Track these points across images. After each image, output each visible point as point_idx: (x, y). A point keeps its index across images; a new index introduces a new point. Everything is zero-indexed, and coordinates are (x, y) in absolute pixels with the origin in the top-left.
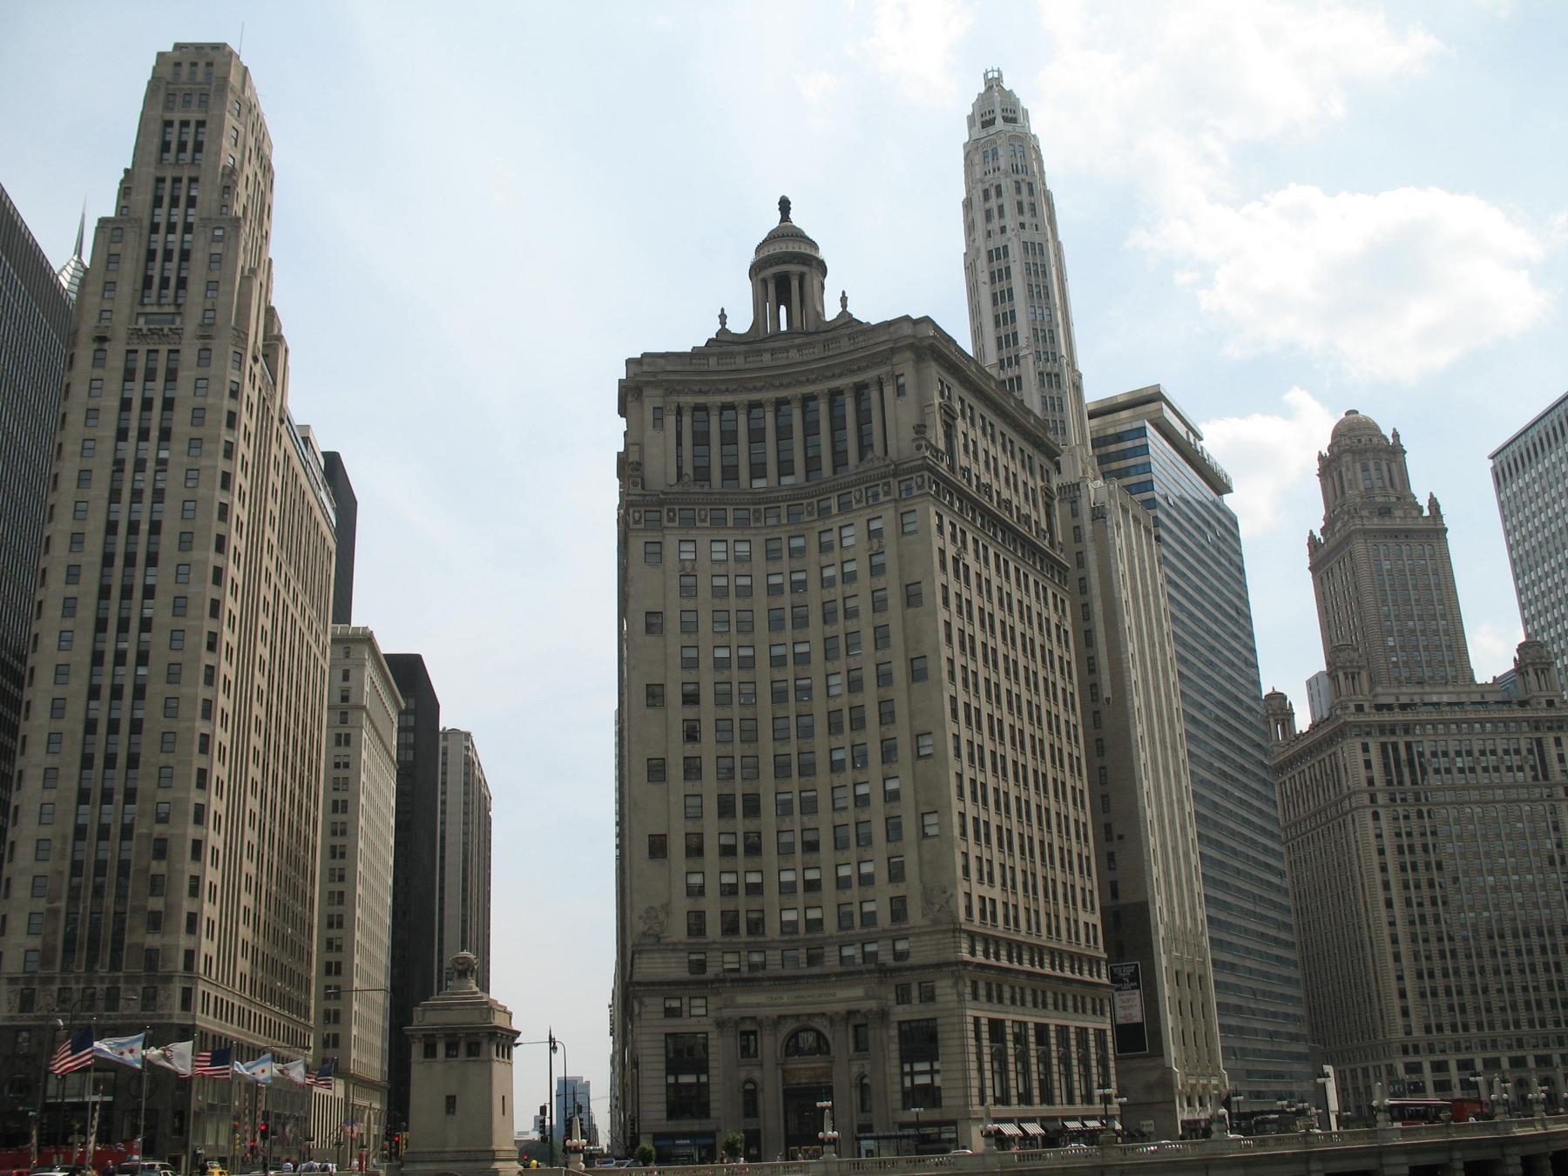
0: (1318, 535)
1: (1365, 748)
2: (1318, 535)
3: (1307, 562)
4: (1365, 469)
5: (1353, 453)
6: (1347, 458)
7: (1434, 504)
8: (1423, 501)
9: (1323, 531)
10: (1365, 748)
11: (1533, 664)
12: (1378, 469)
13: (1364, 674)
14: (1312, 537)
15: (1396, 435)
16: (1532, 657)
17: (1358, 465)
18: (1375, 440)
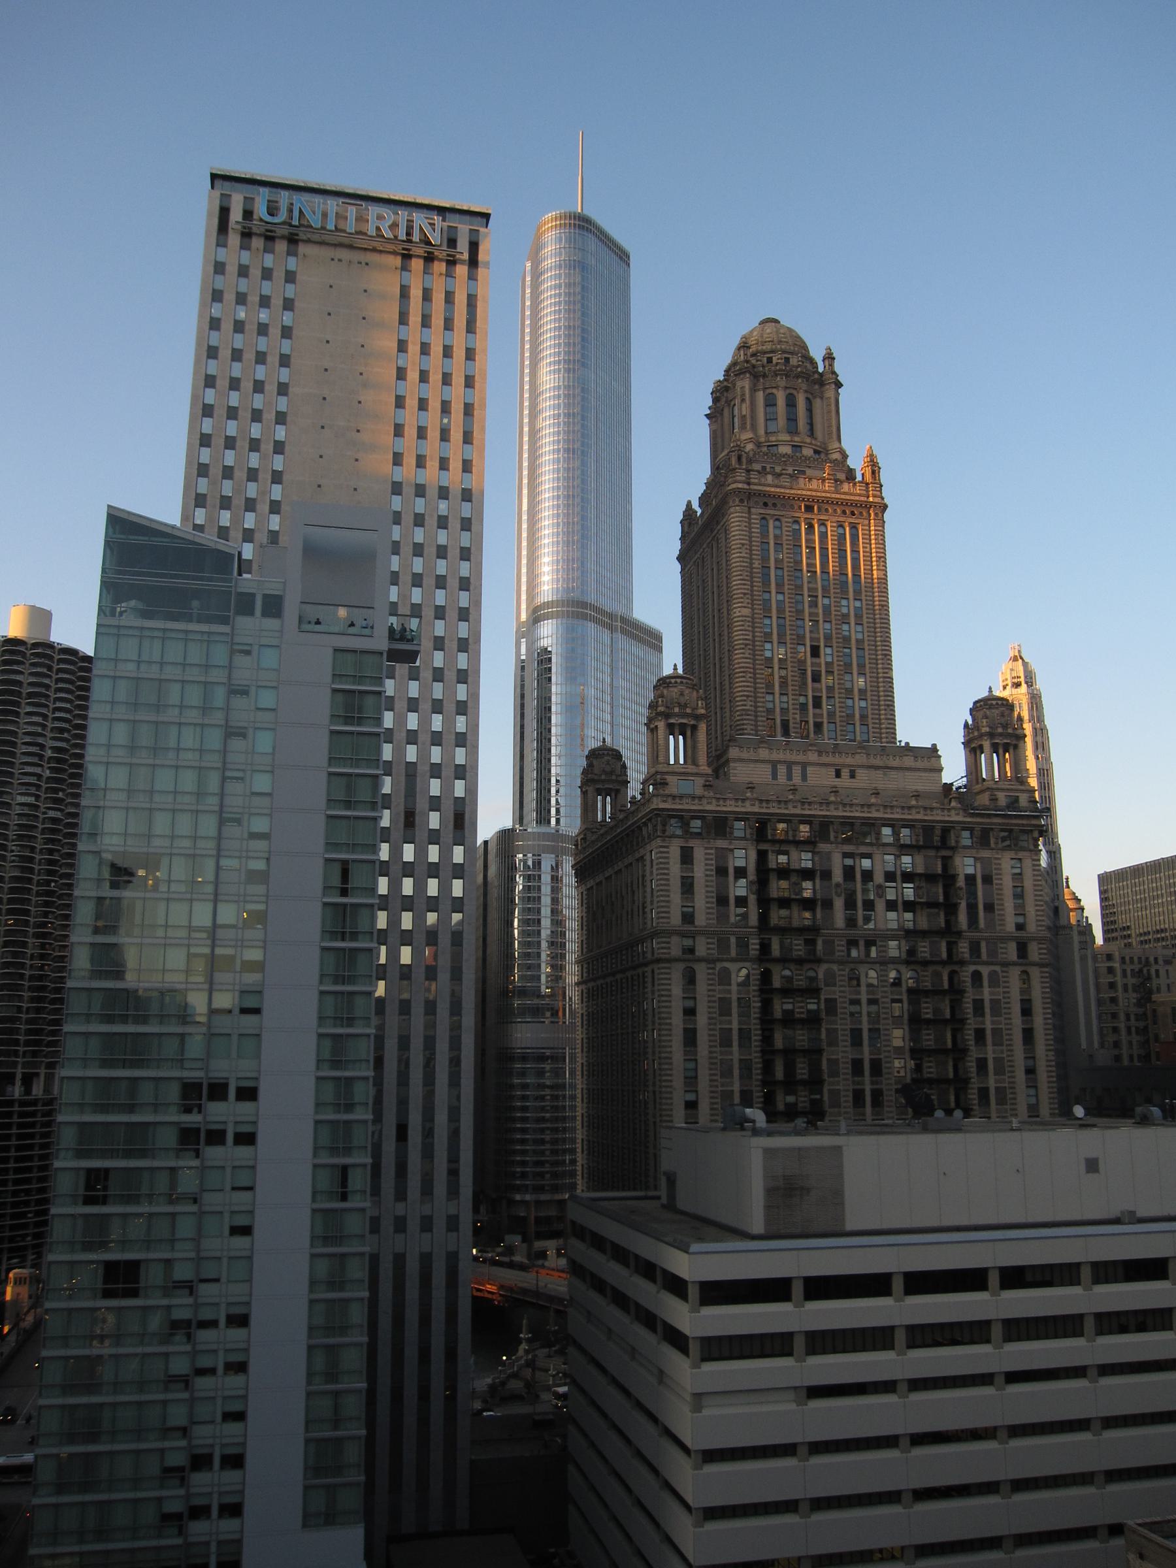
0: (696, 506)
1: (687, 857)
2: (696, 506)
3: (676, 547)
4: (770, 402)
5: (756, 376)
6: (745, 383)
7: (873, 465)
8: (856, 462)
9: (704, 499)
10: (687, 857)
11: (991, 735)
12: (791, 403)
13: (703, 727)
14: (689, 511)
15: (829, 358)
16: (996, 726)
17: (760, 395)
18: (794, 361)
